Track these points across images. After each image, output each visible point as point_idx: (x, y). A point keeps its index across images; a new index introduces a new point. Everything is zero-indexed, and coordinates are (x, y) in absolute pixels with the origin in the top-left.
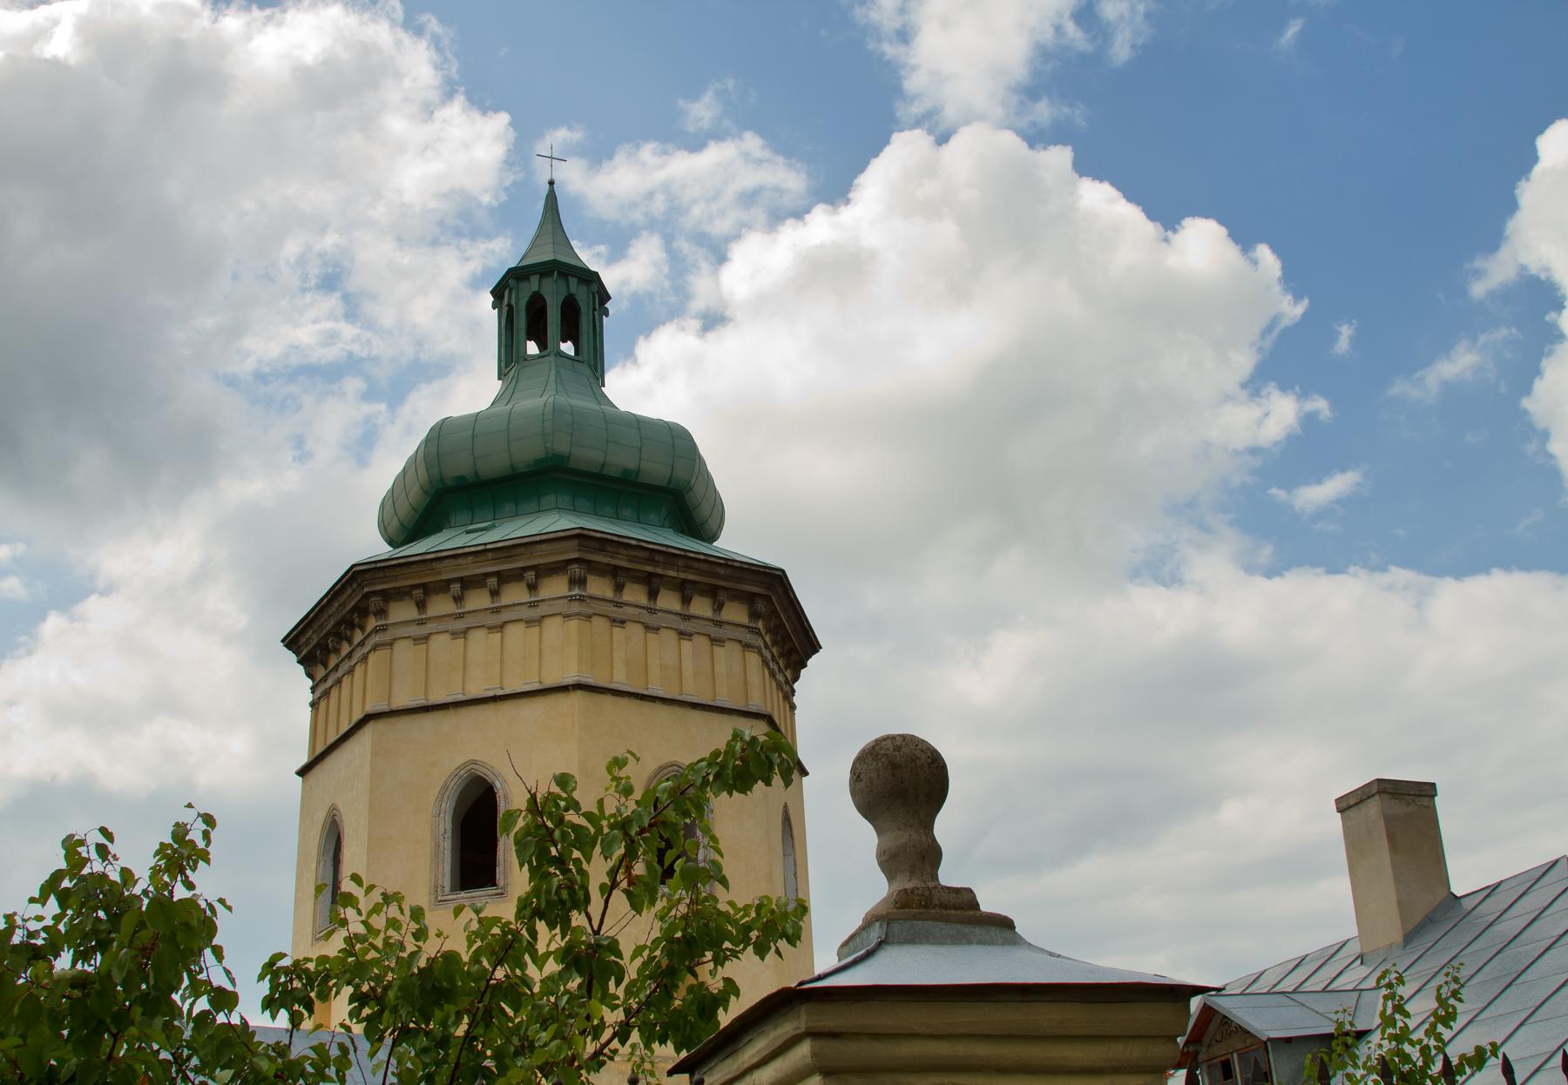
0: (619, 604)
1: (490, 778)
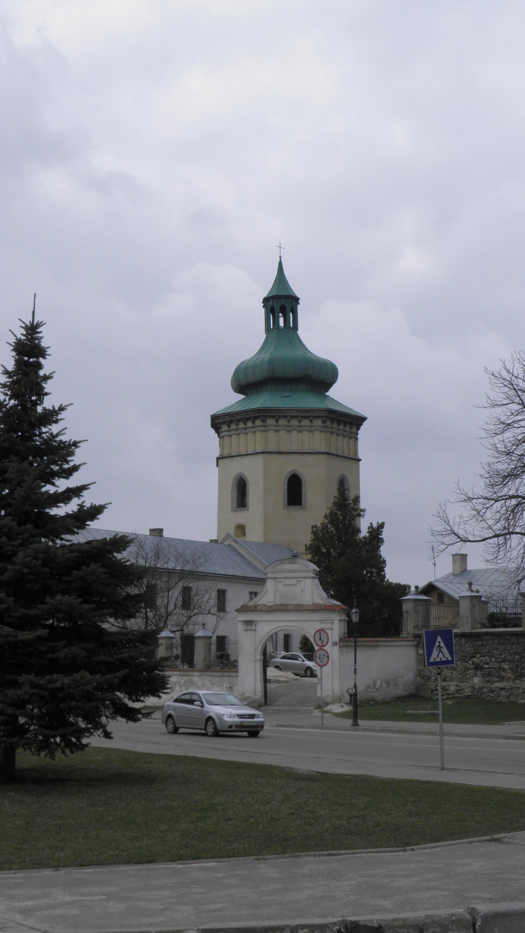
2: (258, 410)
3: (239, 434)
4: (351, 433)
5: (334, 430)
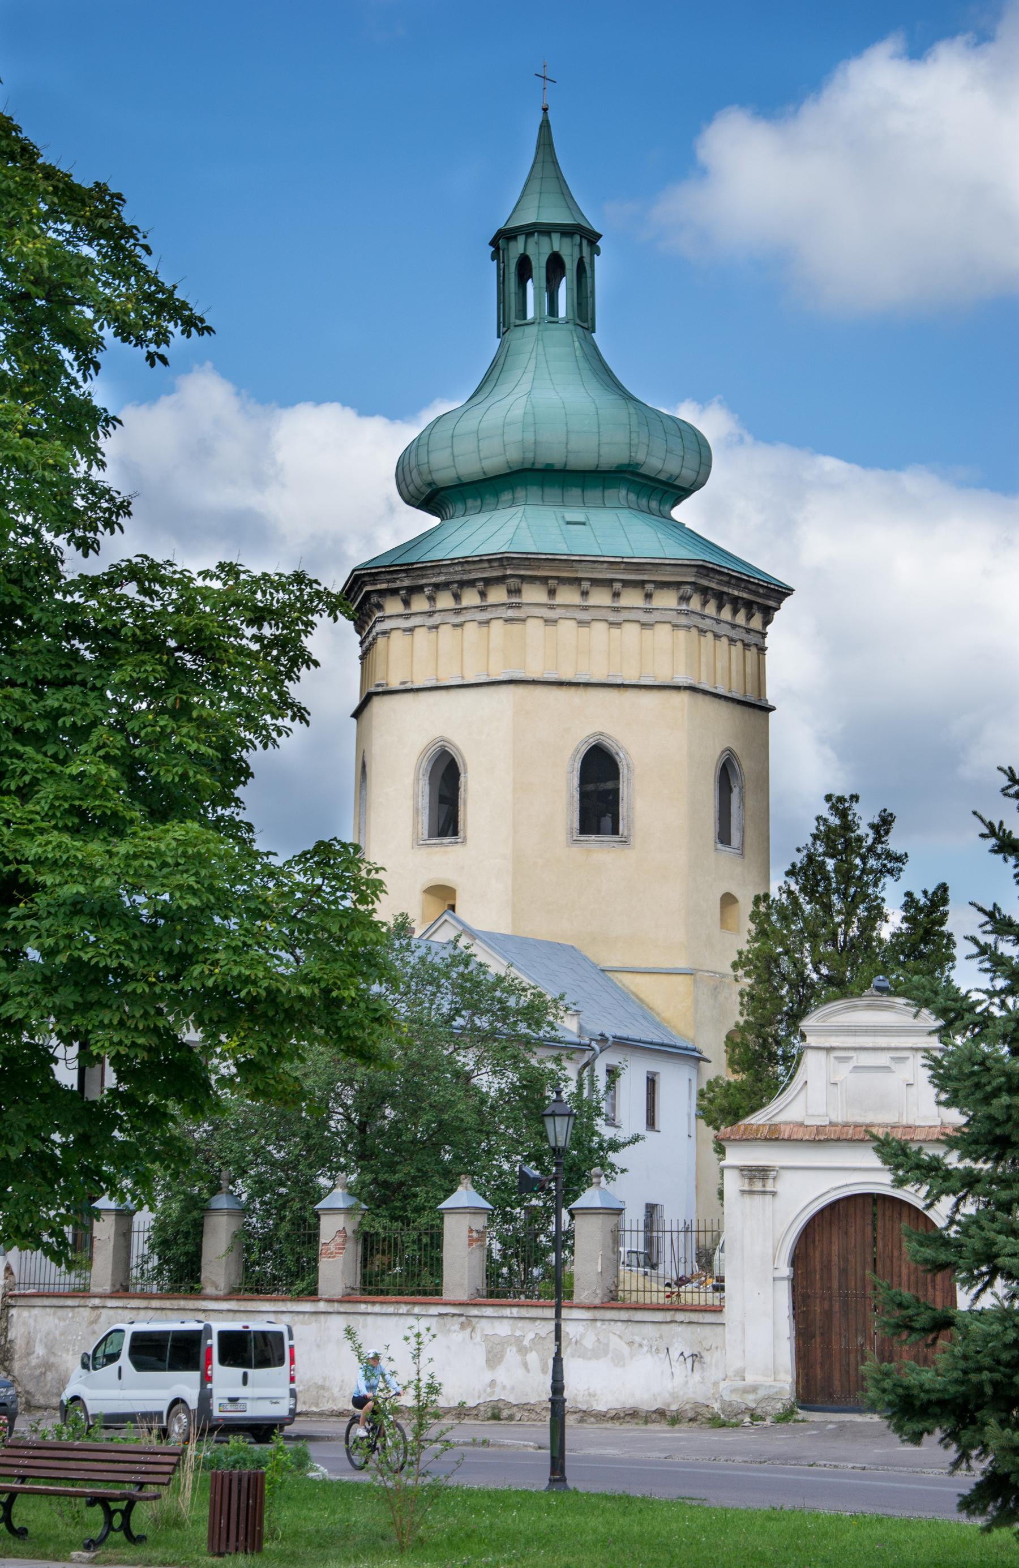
1: (613, 748)
2: (503, 560)
3: (436, 627)
5: (708, 621)
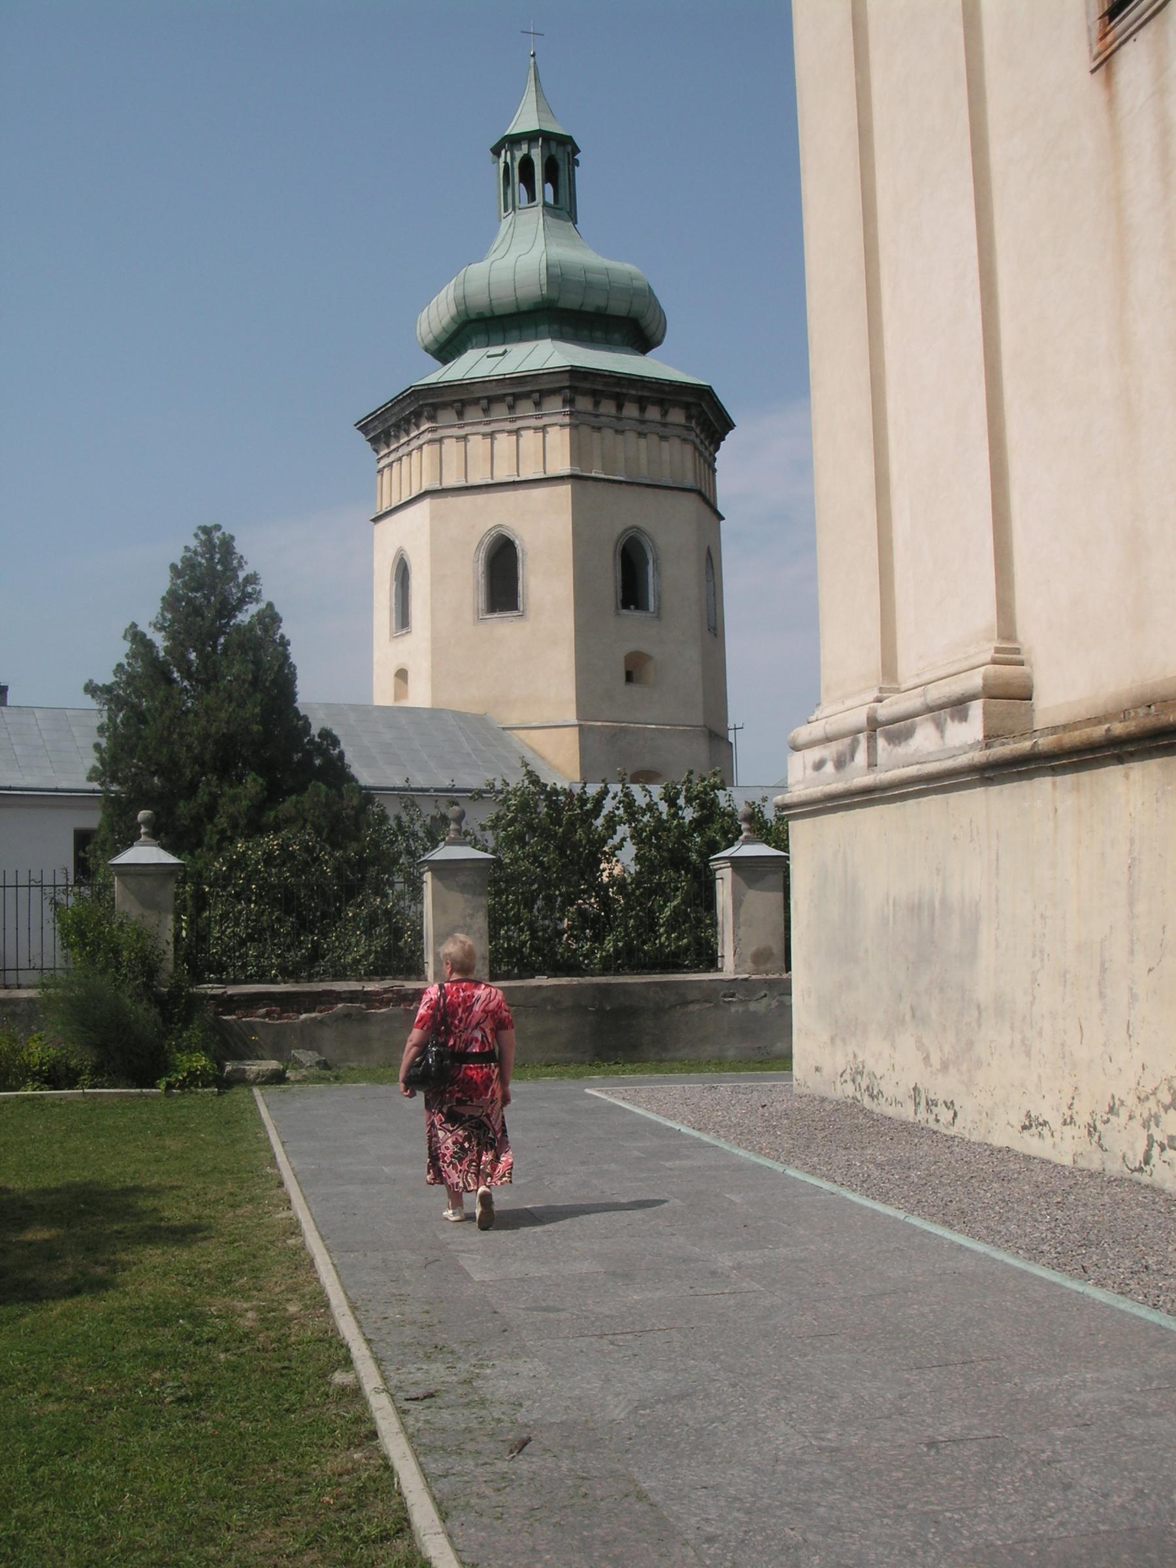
0: (597, 416)
4: (665, 425)
5: (603, 419)
